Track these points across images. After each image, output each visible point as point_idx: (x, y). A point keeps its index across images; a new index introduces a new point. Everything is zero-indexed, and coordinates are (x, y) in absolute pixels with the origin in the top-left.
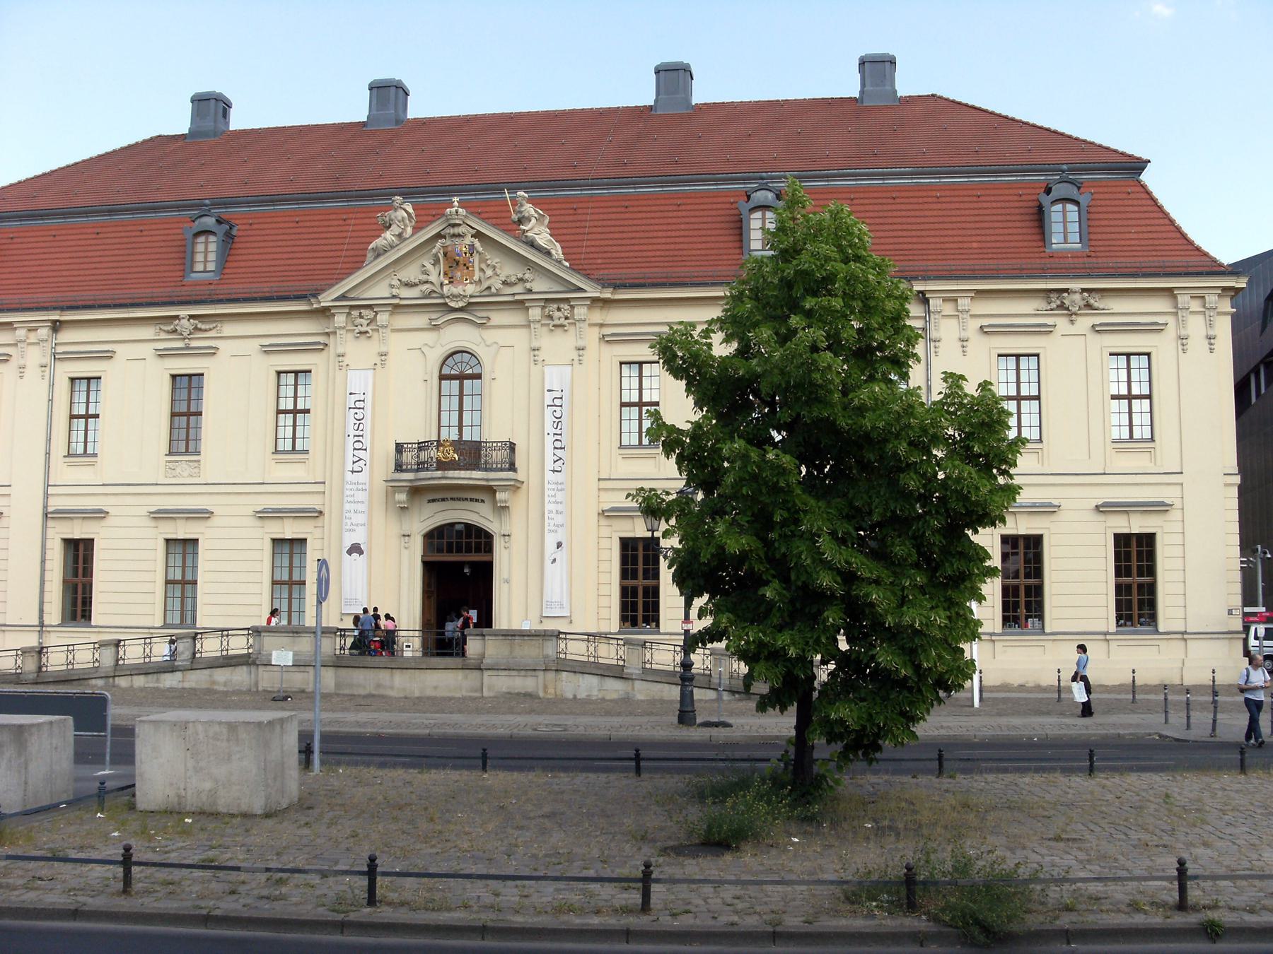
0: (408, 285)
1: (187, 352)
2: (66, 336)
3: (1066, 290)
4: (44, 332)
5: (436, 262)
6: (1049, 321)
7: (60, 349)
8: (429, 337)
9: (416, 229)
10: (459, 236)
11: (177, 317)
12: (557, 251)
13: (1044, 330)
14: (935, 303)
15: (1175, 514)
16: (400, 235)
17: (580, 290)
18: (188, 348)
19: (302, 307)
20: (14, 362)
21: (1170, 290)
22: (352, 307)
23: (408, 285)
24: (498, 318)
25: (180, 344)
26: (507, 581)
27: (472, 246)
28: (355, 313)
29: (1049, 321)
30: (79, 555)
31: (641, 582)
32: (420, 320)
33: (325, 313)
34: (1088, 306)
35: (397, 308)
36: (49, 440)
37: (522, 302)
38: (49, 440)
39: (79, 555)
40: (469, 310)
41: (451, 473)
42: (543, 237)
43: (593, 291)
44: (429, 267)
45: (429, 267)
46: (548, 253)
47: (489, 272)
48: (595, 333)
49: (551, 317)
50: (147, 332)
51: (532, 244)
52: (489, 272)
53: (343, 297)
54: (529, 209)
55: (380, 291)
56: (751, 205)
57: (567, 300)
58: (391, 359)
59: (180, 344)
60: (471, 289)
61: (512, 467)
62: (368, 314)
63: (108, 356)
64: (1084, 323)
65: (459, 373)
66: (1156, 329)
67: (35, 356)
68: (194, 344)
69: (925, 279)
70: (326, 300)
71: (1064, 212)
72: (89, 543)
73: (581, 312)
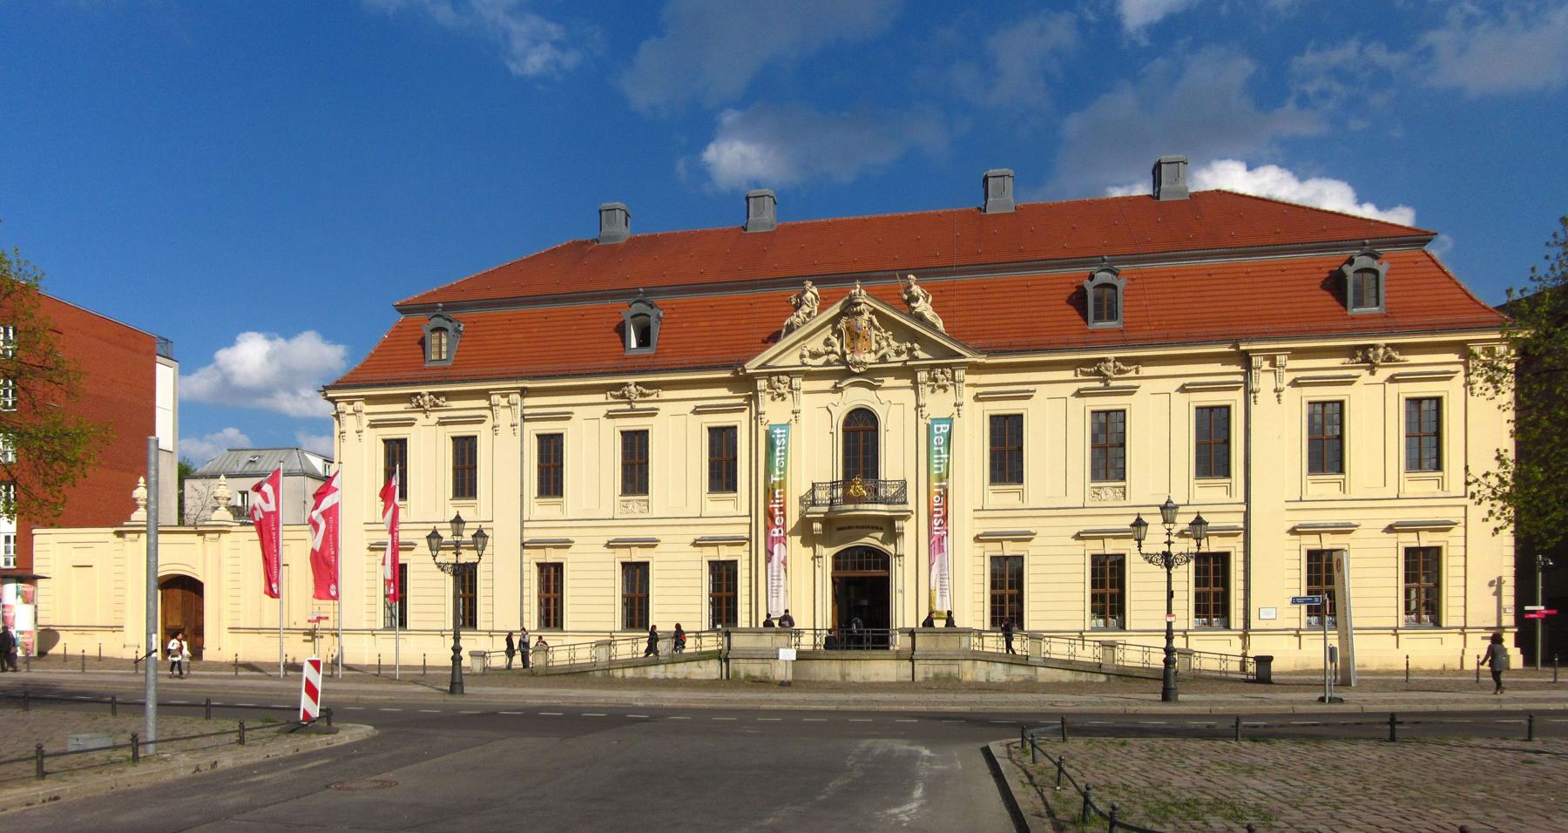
0: (815, 355)
1: (633, 414)
2: (529, 401)
5: (840, 336)
6: (1354, 372)
7: (526, 411)
9: (821, 309)
10: (861, 313)
12: (940, 324)
13: (1348, 381)
14: (1256, 361)
16: (809, 315)
19: (727, 374)
20: (489, 422)
22: (771, 374)
23: (815, 355)
24: (889, 381)
25: (628, 407)
26: (902, 592)
27: (871, 321)
28: (775, 378)
29: (1354, 372)
30: (551, 577)
32: (828, 384)
34: (1390, 359)
35: (809, 376)
37: (912, 367)
39: (551, 577)
40: (871, 378)
41: (861, 506)
42: (929, 314)
43: (970, 358)
44: (834, 339)
45: (834, 339)
46: (933, 327)
47: (884, 343)
48: (968, 394)
49: (936, 380)
51: (920, 318)
52: (884, 343)
53: (763, 366)
54: (916, 290)
55: (791, 360)
56: (1096, 282)
57: (949, 366)
58: (802, 416)
60: (870, 358)
61: (905, 502)
62: (785, 379)
63: (566, 417)
64: (1383, 373)
66: (1447, 377)
68: (638, 406)
69: (1250, 340)
70: (751, 367)
73: (960, 374)
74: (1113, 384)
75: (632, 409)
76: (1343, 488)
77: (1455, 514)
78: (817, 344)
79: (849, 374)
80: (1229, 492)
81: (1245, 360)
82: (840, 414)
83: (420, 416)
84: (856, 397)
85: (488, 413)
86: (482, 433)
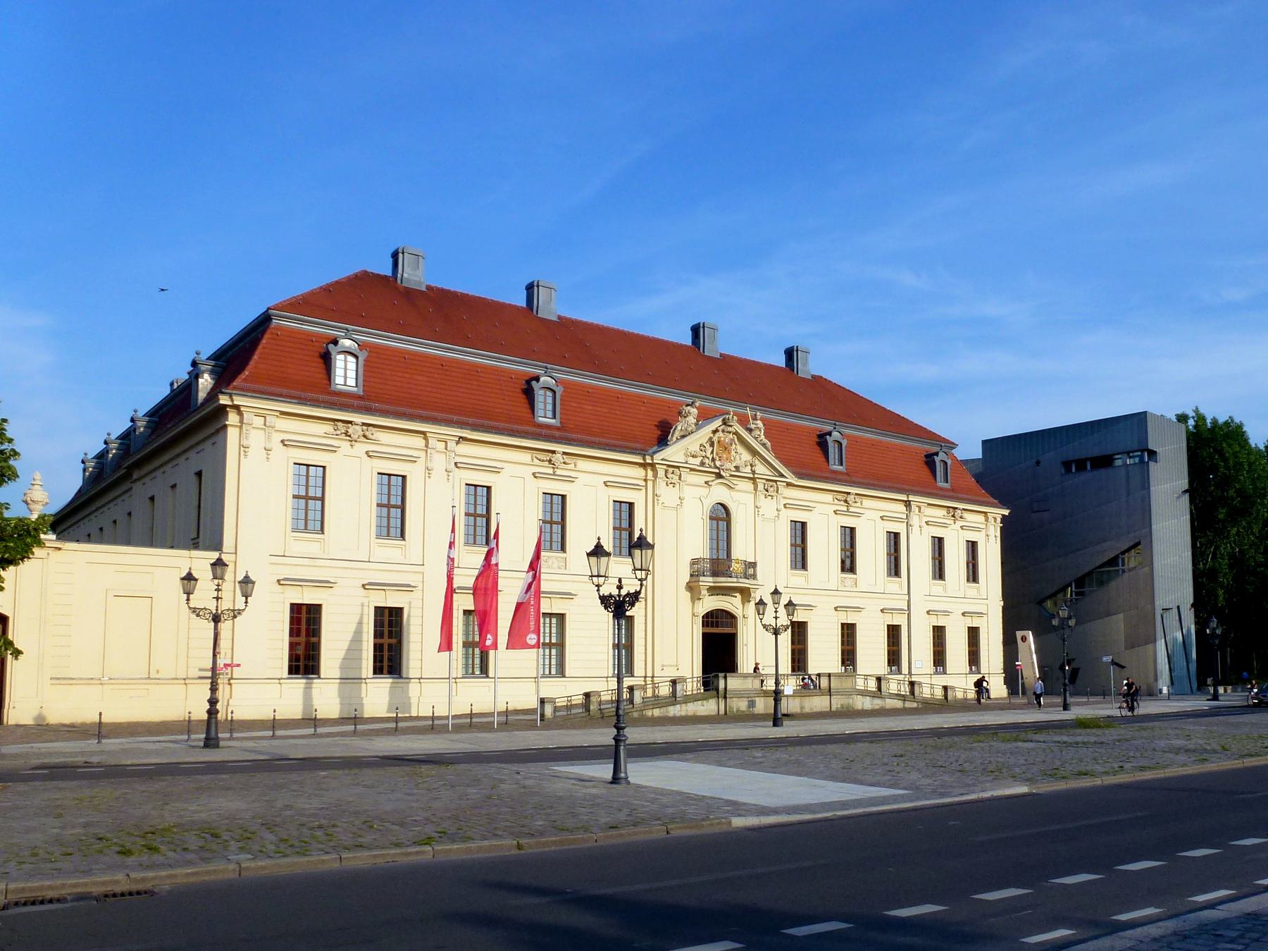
1: (554, 477)
2: (465, 449)
3: (350, 422)
4: (451, 445)
5: (712, 445)
8: (705, 491)
11: (554, 452)
15: (417, 594)
17: (782, 476)
18: (554, 474)
21: (424, 433)
28: (671, 470)
31: (386, 641)
32: (701, 479)
33: (653, 466)
36: (453, 531)
38: (453, 531)
43: (791, 478)
45: (707, 446)
50: (526, 457)
59: (551, 471)
63: (496, 471)
65: (721, 517)
67: (439, 462)
70: (658, 458)
71: (346, 361)
72: (399, 611)
74: (851, 509)
75: (554, 474)
76: (945, 590)
77: (982, 609)
78: (695, 448)
79: (719, 476)
80: (901, 587)
81: (908, 504)
82: (709, 503)
83: (345, 445)
84: (719, 493)
85: (422, 454)
86: (415, 475)
